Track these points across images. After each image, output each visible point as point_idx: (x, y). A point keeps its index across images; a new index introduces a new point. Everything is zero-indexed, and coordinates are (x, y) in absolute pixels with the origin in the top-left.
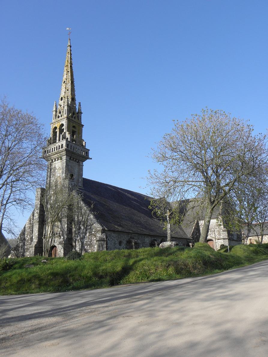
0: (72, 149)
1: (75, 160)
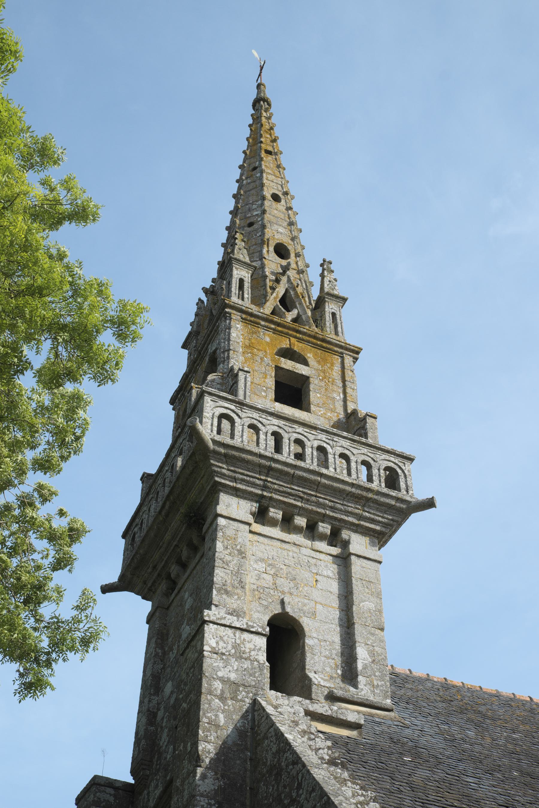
1: (301, 521)
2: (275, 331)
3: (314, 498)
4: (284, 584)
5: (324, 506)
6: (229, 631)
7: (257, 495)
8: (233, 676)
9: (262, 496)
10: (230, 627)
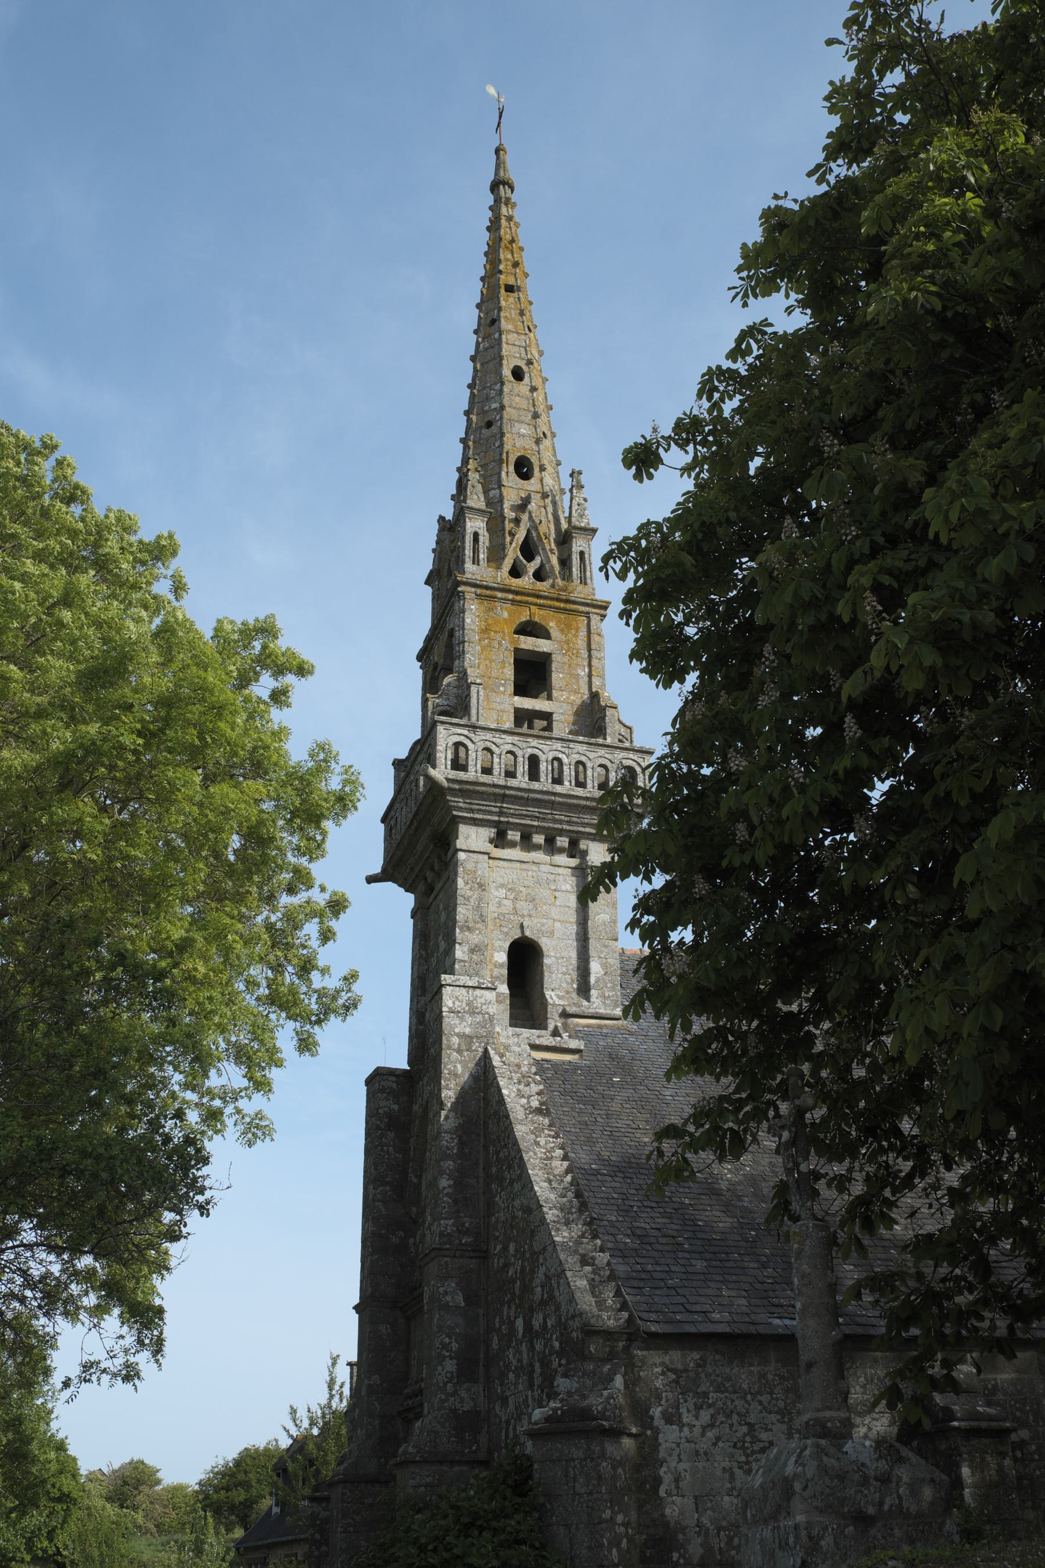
0: (522, 768)
1: (539, 839)
2: (513, 602)
3: (550, 816)
4: (523, 906)
5: (561, 822)
6: (464, 991)
7: (494, 821)
8: (467, 1031)
9: (500, 822)
10: (464, 986)
